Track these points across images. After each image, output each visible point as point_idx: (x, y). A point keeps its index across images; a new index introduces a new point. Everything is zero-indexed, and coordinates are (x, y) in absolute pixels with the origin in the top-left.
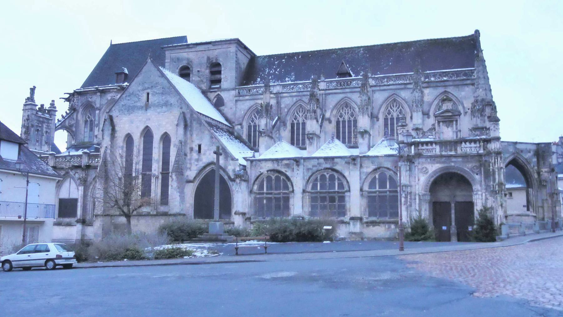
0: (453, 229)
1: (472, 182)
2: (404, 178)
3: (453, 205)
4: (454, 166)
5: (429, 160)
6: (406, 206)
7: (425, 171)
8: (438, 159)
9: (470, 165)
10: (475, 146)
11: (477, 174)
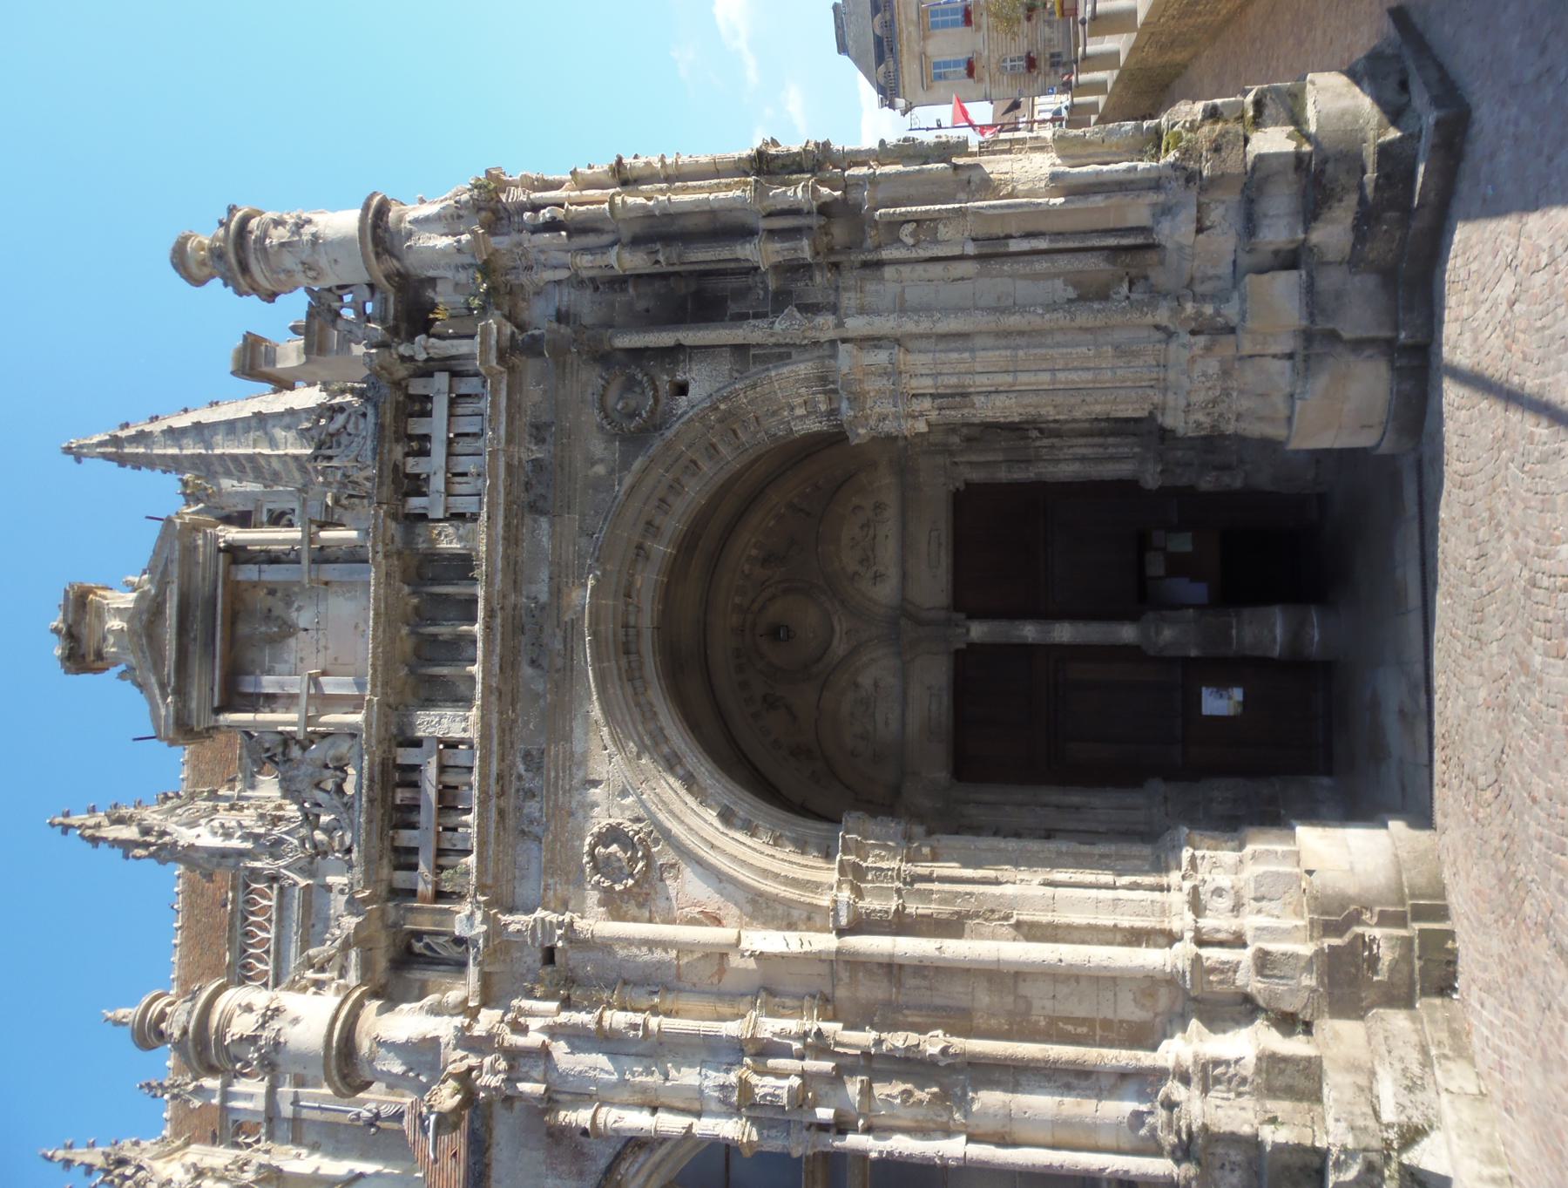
0: (1168, 634)
3: (978, 631)
5: (532, 807)
10: (440, 407)
11: (682, 389)
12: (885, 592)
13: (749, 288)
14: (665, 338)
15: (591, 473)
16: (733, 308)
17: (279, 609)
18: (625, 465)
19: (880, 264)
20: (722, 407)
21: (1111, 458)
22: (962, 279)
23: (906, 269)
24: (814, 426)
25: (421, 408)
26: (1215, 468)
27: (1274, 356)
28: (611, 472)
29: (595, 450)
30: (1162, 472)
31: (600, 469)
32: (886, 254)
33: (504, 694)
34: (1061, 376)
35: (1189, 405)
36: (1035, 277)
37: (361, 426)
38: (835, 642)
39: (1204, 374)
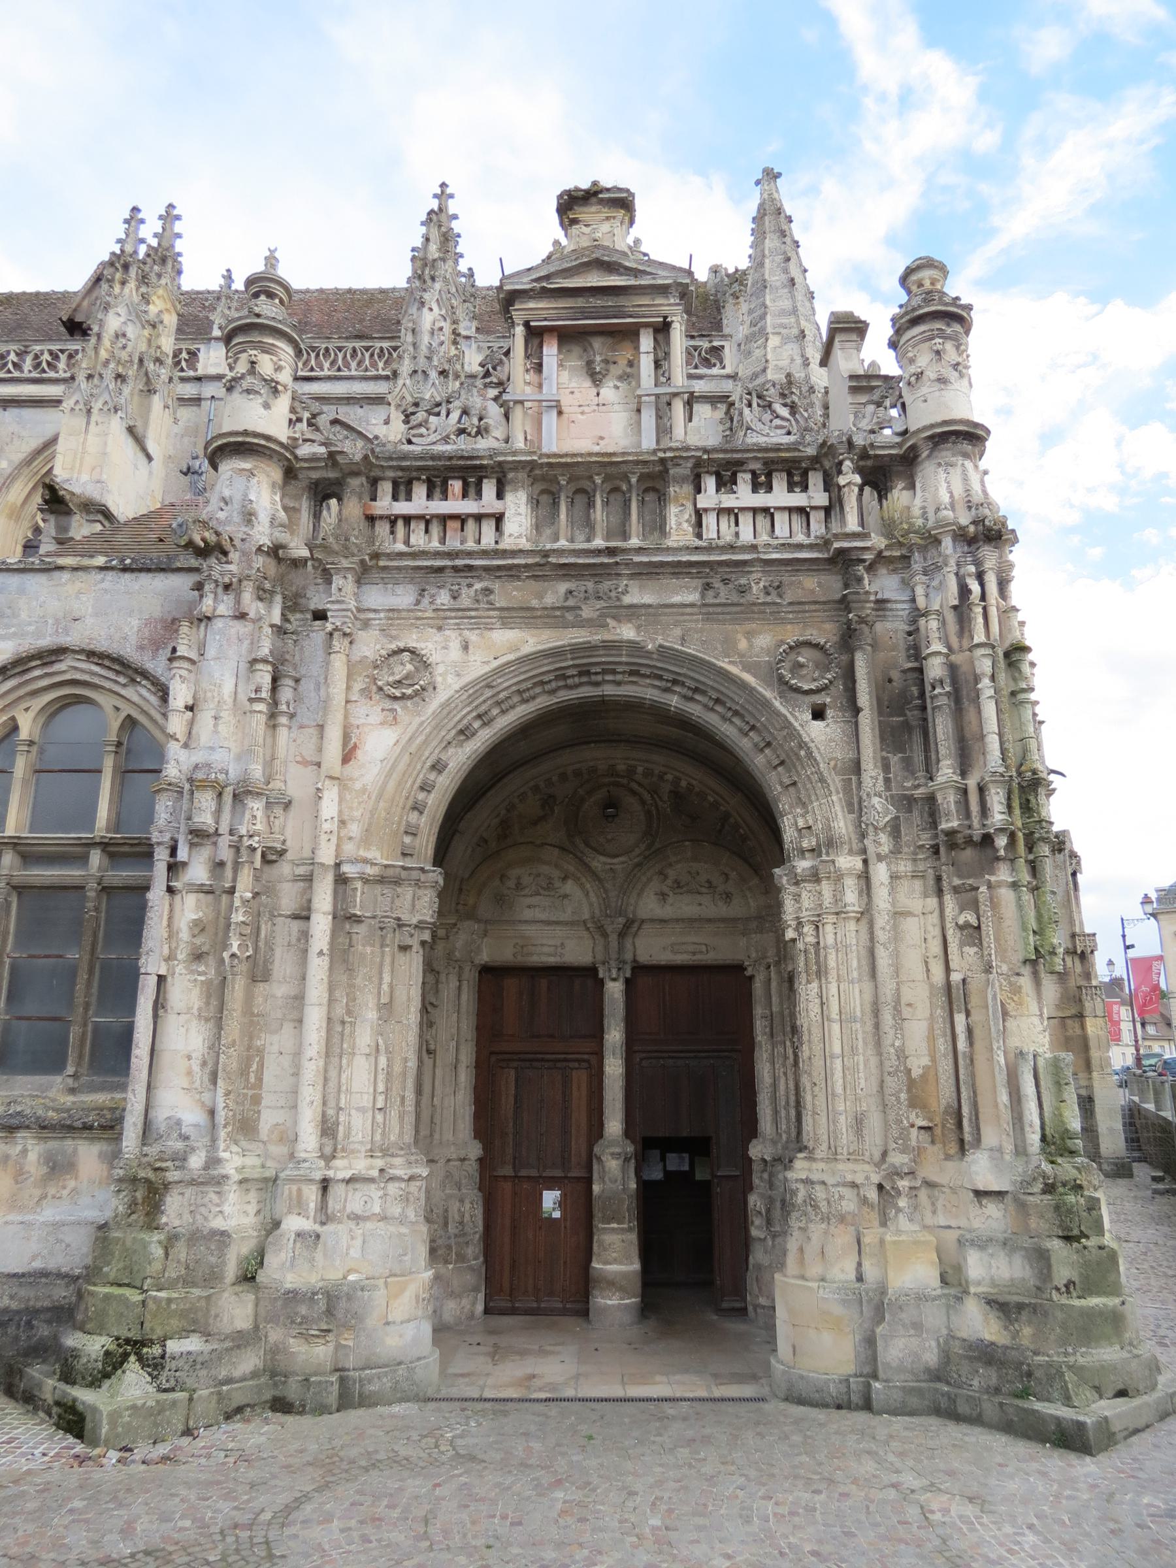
0: (613, 1165)
1: (774, 783)
2: (212, 719)
3: (615, 990)
4: (635, 648)
5: (443, 598)
6: (208, 970)
7: (403, 682)
8: (507, 593)
9: (763, 641)
10: (798, 499)
11: (818, 714)
12: (649, 905)
13: (913, 773)
14: (864, 698)
15: (739, 636)
16: (895, 759)
17: (615, 370)
18: (747, 668)
19: (940, 893)
20: (802, 753)
21: (776, 1112)
22: (928, 970)
23: (934, 918)
24: (789, 834)
25: (798, 483)
26: (768, 1211)
27: (859, 1264)
28: (742, 656)
29: (763, 641)
30: (764, 1161)
31: (743, 644)
32: (948, 898)
33: (542, 567)
34: (838, 1063)
35: (812, 1183)
36: (931, 1038)
37: (779, 431)
38: (603, 859)
39: (841, 1197)
